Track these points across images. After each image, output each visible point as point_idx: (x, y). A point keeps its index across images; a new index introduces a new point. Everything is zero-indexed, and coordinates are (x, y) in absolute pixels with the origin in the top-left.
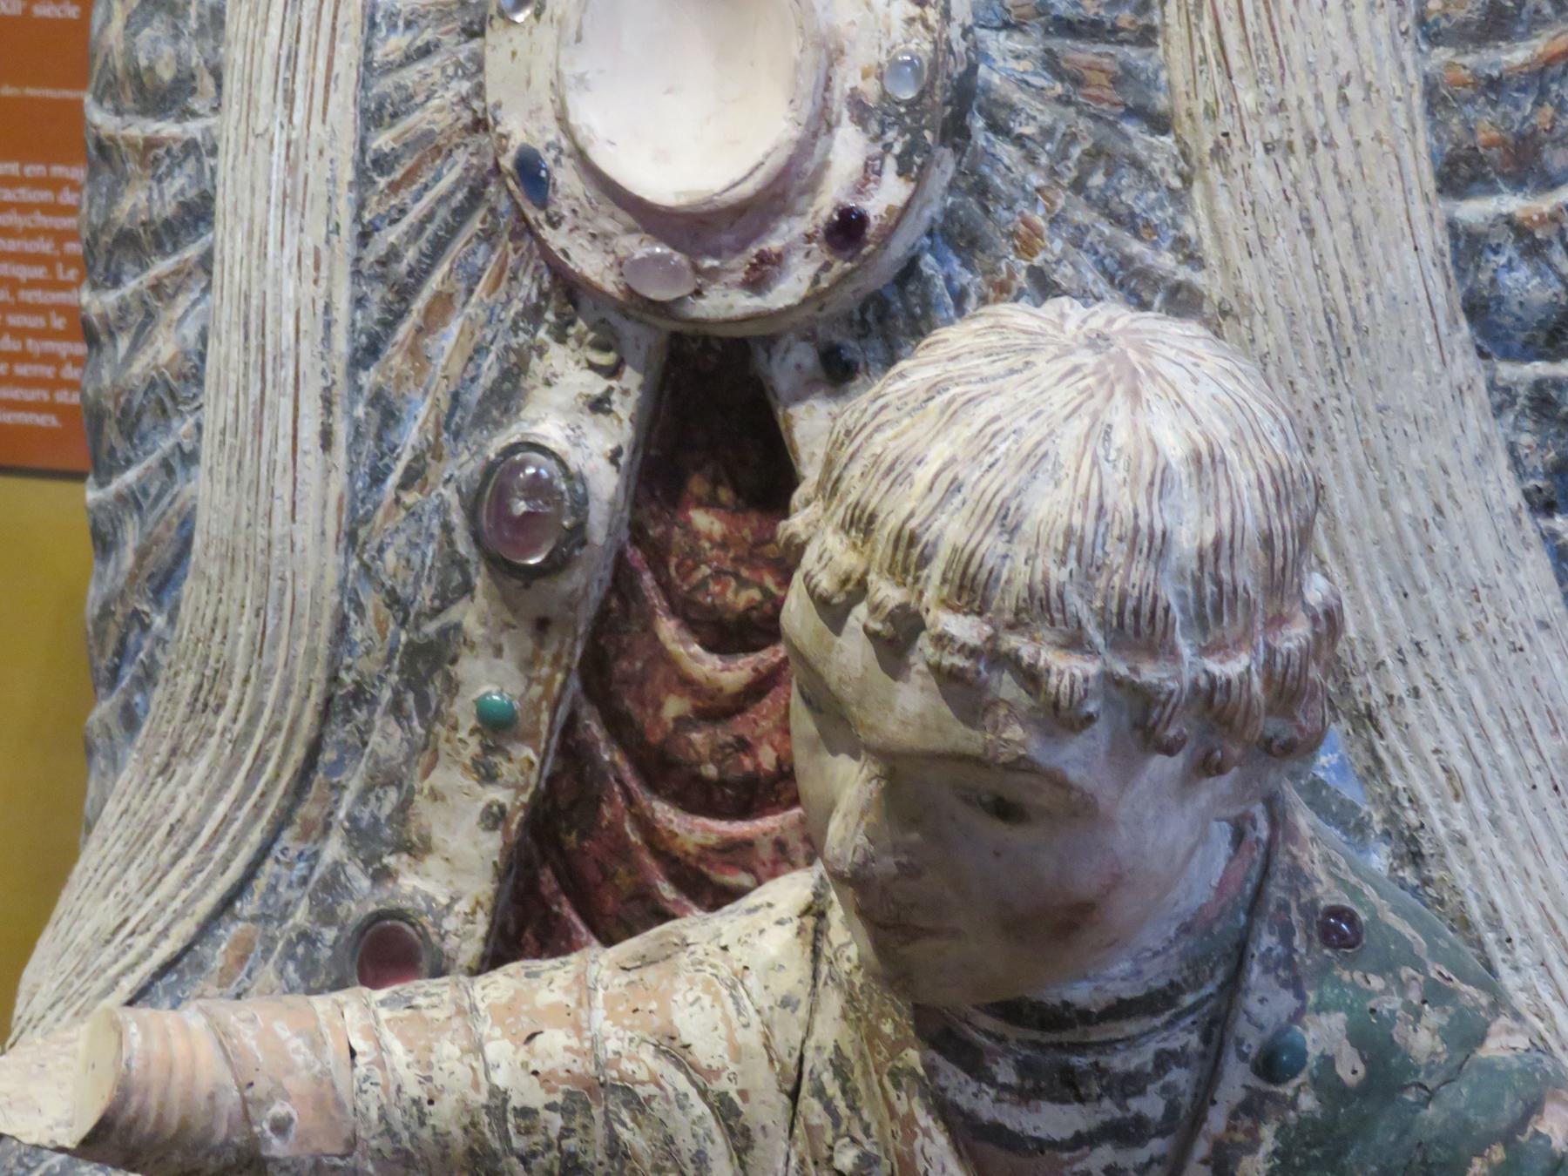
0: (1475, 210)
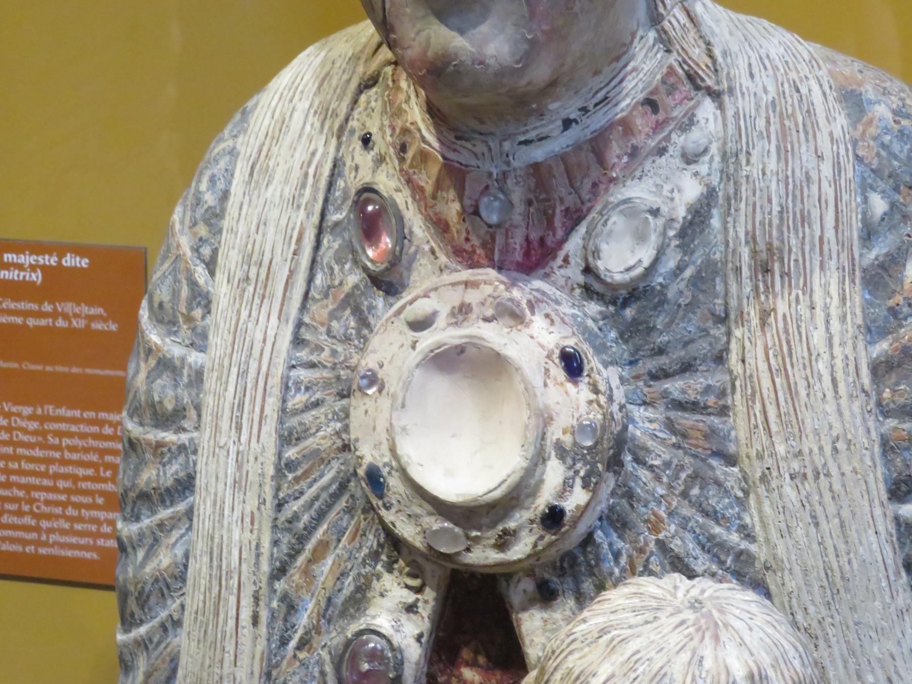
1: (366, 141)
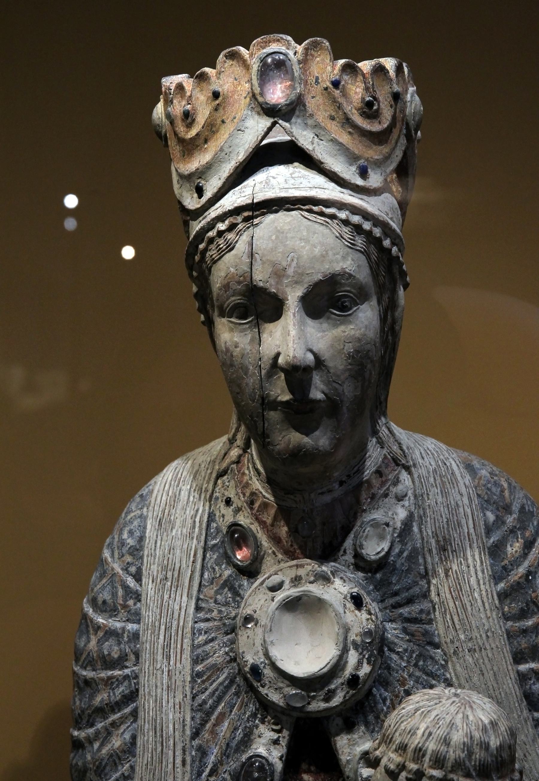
0: (523, 667)
1: (228, 502)
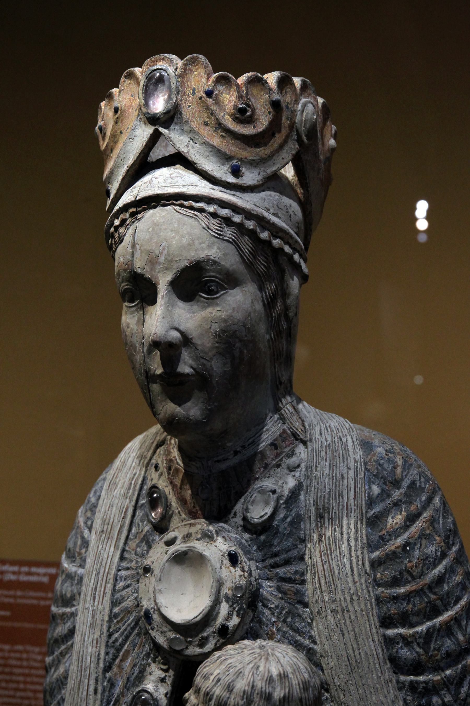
0: (391, 632)
1: (156, 468)
